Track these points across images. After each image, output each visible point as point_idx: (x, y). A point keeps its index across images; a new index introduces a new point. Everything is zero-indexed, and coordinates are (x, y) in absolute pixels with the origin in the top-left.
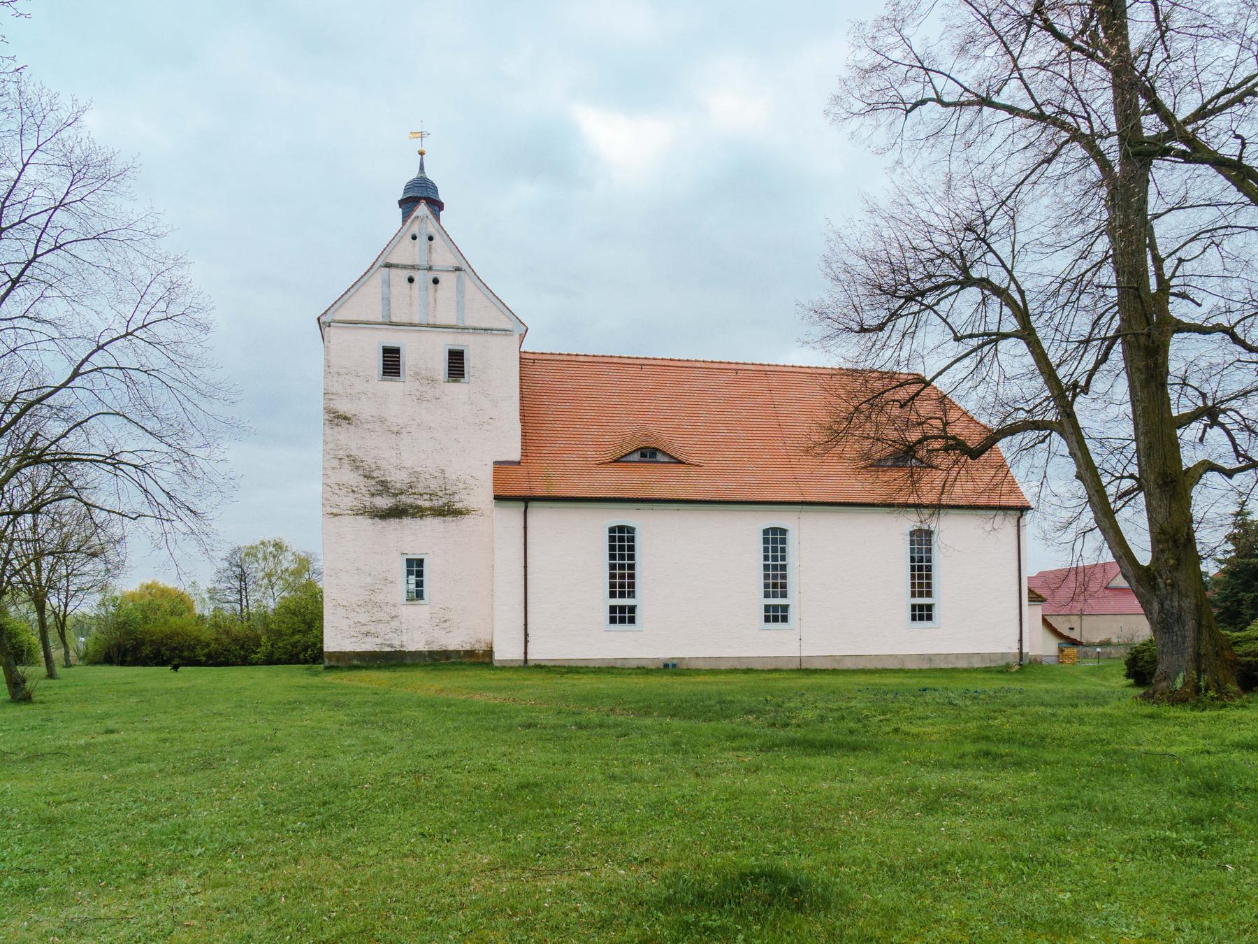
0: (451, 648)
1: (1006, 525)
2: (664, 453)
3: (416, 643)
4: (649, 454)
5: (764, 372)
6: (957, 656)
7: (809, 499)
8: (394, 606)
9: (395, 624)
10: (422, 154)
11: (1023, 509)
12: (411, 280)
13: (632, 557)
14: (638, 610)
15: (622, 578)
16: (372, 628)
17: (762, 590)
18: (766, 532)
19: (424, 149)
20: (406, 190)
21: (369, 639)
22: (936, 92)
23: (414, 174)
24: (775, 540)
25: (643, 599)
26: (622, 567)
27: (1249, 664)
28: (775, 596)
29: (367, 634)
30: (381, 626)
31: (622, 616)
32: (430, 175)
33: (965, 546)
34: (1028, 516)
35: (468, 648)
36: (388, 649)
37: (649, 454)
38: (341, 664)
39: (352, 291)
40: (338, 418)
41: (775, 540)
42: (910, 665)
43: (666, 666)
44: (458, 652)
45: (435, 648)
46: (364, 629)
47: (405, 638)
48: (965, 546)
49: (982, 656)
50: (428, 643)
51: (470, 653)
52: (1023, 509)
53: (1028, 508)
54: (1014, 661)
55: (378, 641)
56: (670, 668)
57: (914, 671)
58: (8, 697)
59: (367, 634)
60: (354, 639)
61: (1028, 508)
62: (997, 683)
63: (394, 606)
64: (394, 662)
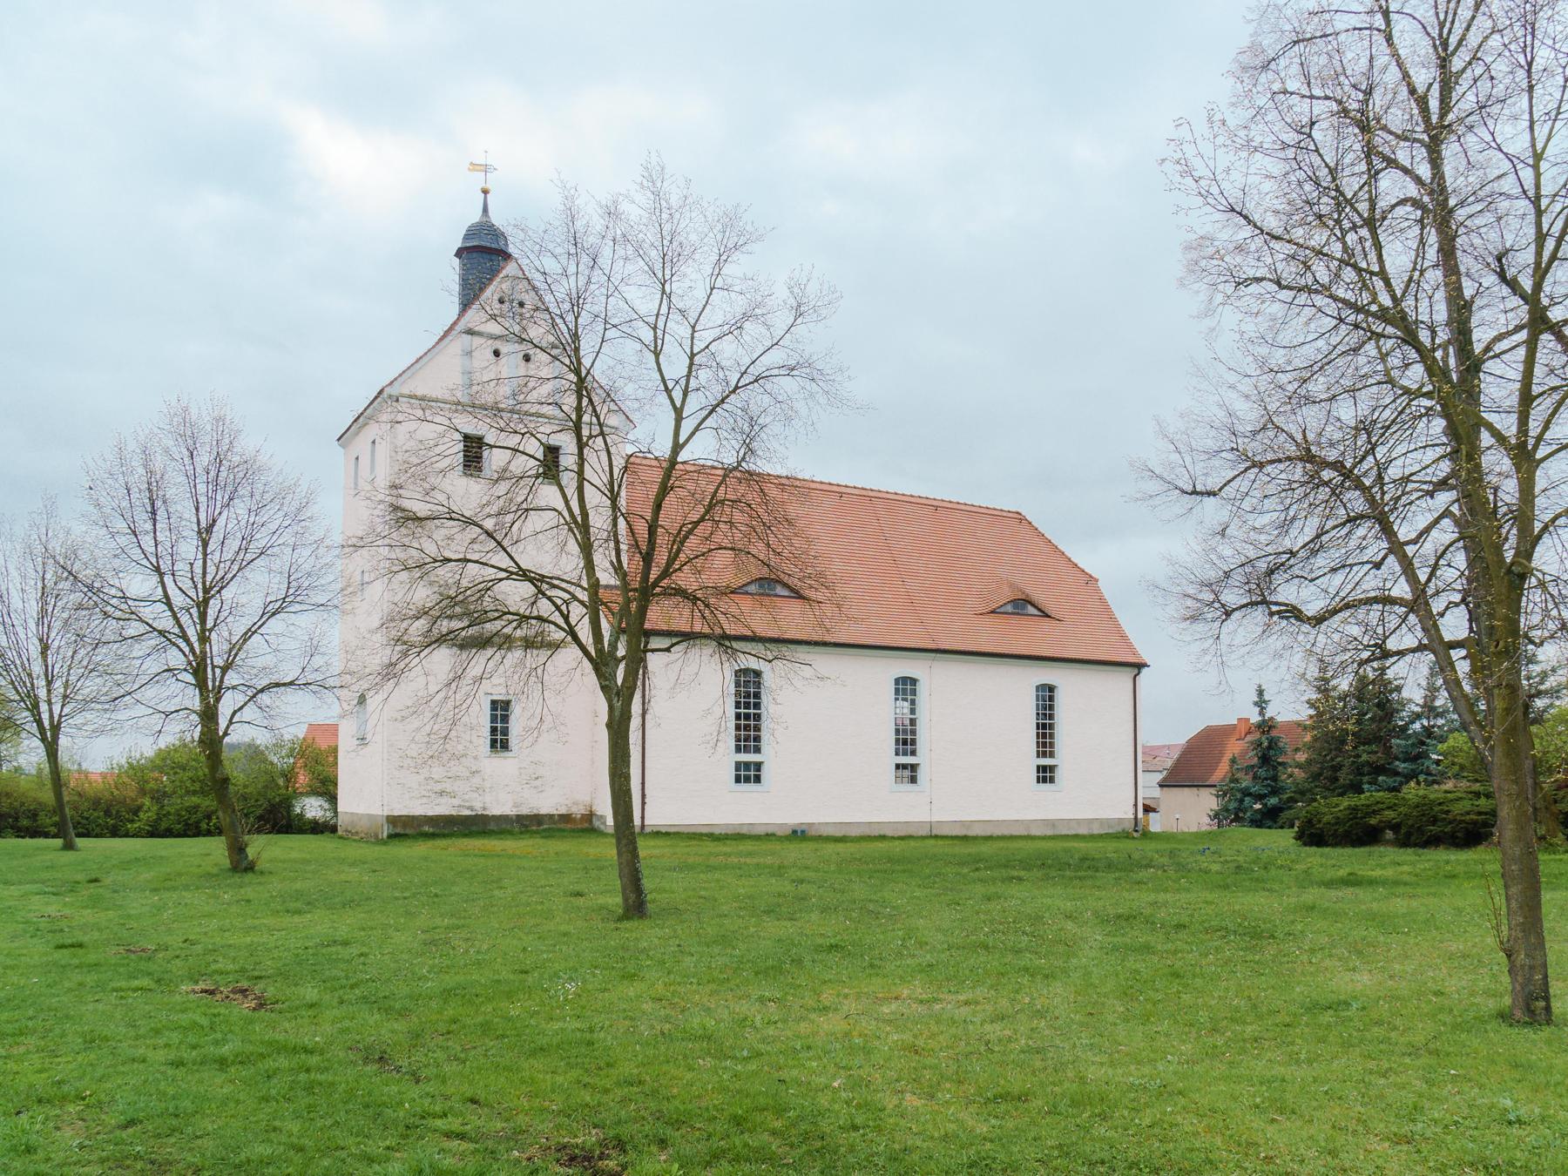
0: (543, 812)
1: (1123, 679)
2: (1033, 605)
3: (500, 805)
4: (1022, 604)
5: (869, 498)
6: (1078, 821)
7: (942, 647)
8: (475, 758)
9: (476, 780)
10: (485, 192)
11: (1139, 666)
12: (497, 353)
13: (757, 706)
14: (764, 768)
15: (748, 730)
16: (447, 786)
17: (893, 747)
18: (897, 681)
19: (488, 186)
20: (466, 237)
21: (444, 800)
22: (1532, 346)
23: (475, 217)
24: (1047, 695)
25: (770, 755)
26: (747, 717)
27: (1475, 823)
28: (905, 754)
29: (442, 793)
30: (458, 783)
31: (749, 774)
32: (497, 219)
33: (1086, 701)
34: (1145, 671)
35: (563, 811)
36: (467, 813)
37: (1022, 604)
38: (408, 831)
39: (425, 360)
40: (406, 518)
41: (1047, 695)
42: (1035, 832)
43: (795, 832)
44: (551, 816)
45: (525, 811)
46: (438, 788)
47: (488, 798)
48: (1086, 701)
49: (1101, 822)
50: (516, 805)
51: (566, 818)
52: (1139, 666)
53: (1145, 665)
54: (1129, 826)
55: (456, 802)
56: (798, 835)
57: (1101, 836)
58: (227, 863)
59: (442, 793)
60: (425, 800)
61: (1145, 665)
62: (1111, 846)
63: (475, 758)
64: (474, 828)
